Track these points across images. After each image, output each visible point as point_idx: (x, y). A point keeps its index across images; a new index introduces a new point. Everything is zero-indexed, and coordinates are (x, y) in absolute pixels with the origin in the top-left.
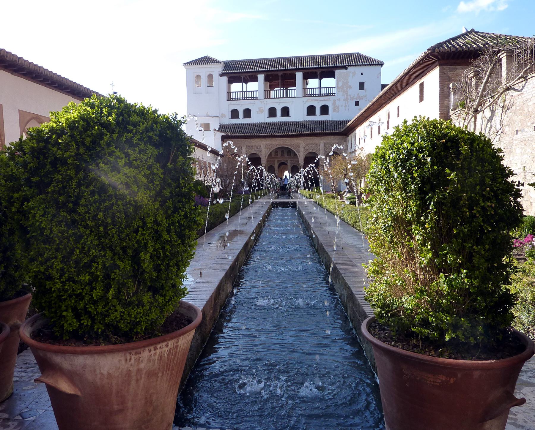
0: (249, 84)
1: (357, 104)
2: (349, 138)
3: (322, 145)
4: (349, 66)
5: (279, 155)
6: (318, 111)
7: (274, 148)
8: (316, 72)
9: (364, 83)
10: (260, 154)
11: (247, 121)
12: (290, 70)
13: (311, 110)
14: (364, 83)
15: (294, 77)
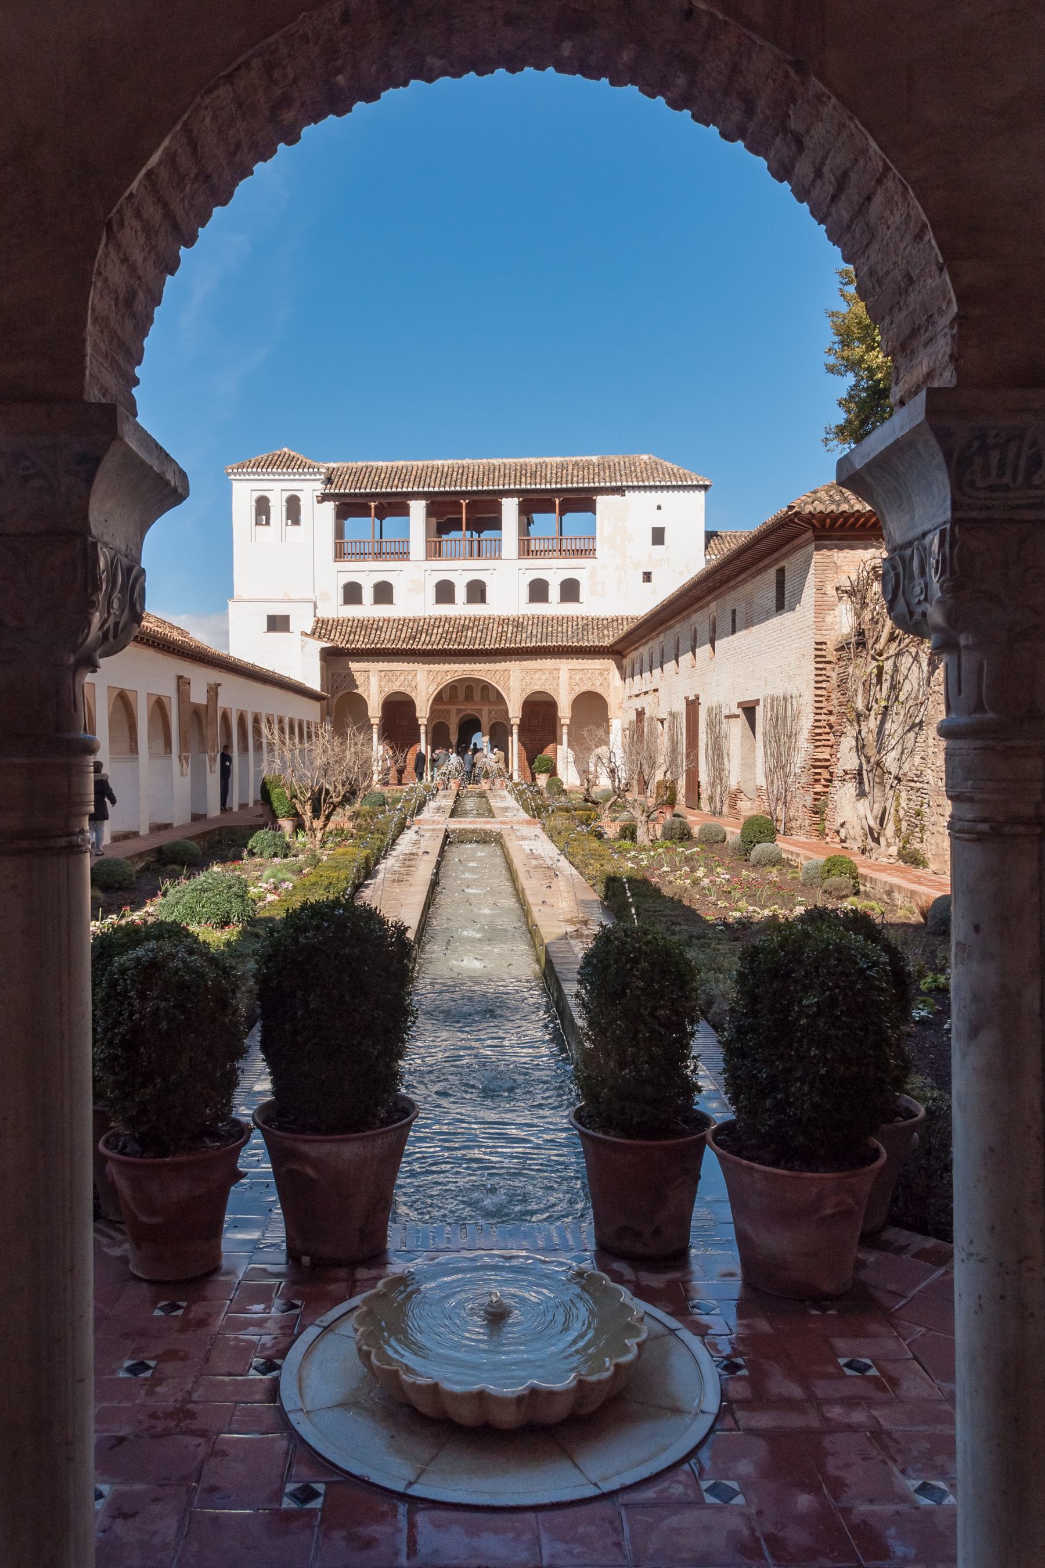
0: (389, 521)
1: (647, 577)
2: (626, 662)
3: (564, 675)
4: (628, 487)
5: (461, 696)
6: (554, 592)
7: (448, 679)
8: (550, 500)
9: (663, 529)
10: (413, 695)
11: (383, 611)
12: (488, 492)
13: (538, 591)
14: (663, 529)
15: (498, 508)
